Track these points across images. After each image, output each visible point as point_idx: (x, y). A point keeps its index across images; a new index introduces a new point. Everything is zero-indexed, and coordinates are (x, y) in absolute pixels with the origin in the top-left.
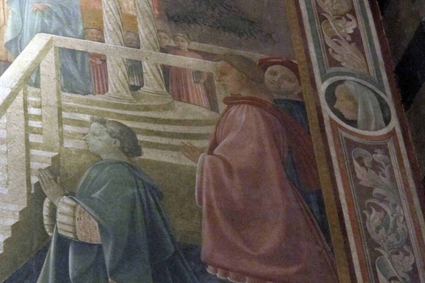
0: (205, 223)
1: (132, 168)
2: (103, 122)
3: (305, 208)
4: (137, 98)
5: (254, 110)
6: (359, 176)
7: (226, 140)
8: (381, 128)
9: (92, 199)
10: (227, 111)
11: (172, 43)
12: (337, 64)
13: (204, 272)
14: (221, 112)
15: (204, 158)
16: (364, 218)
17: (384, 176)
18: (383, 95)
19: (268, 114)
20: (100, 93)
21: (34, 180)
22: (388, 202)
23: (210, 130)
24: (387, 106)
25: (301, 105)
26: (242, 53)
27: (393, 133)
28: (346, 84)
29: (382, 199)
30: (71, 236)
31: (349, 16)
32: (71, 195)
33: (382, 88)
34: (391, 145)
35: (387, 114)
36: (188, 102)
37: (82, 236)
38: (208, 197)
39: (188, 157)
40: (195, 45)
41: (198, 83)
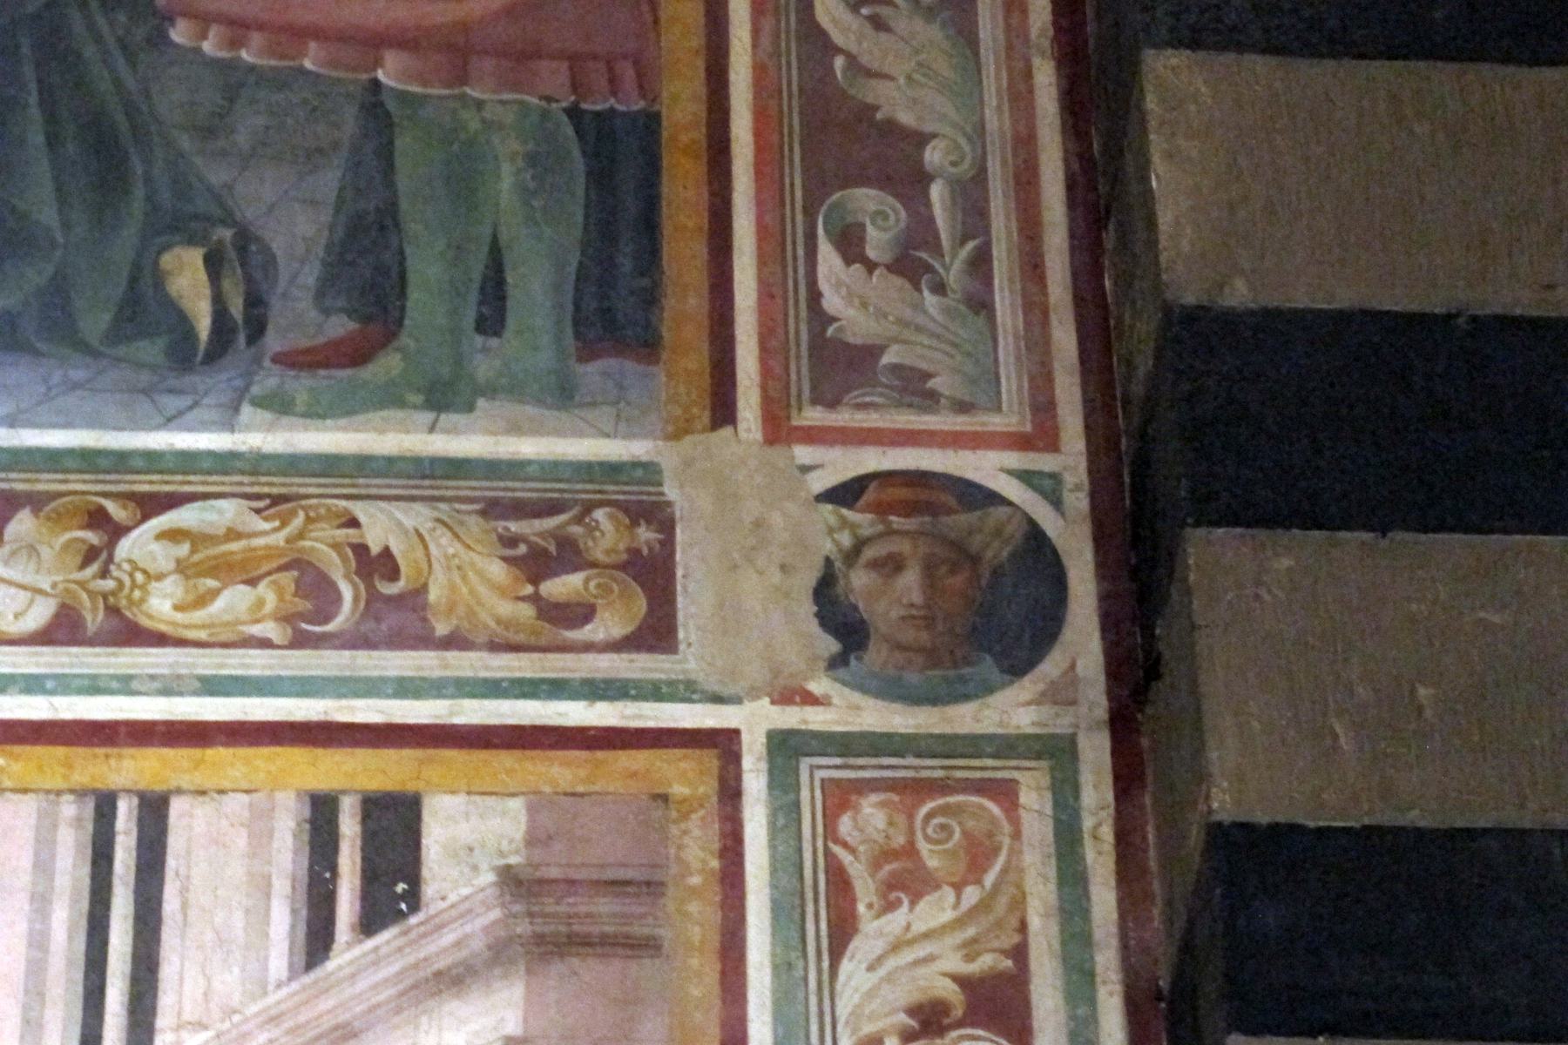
13: (159, 39)
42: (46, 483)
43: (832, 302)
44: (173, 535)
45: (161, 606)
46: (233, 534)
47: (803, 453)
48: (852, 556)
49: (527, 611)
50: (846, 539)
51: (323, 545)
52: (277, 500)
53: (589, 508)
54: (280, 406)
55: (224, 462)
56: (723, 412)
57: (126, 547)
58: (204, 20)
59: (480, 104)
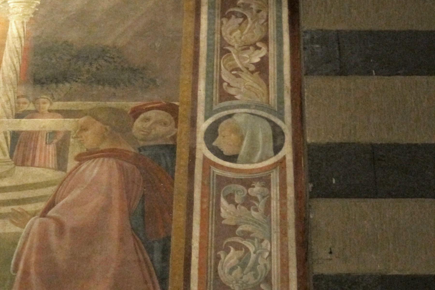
3: (145, 259)
5: (112, 162)
6: (223, 214)
7: (68, 198)
8: (268, 158)
10: (76, 168)
12: (232, 97)
14: (69, 170)
16: (218, 258)
17: (256, 210)
18: (279, 122)
22: (253, 238)
23: (49, 191)
24: (282, 134)
26: (113, 104)
27: (282, 161)
28: (235, 117)
29: (247, 235)
33: (281, 115)
35: (279, 142)
38: (26, 264)
40: (57, 105)
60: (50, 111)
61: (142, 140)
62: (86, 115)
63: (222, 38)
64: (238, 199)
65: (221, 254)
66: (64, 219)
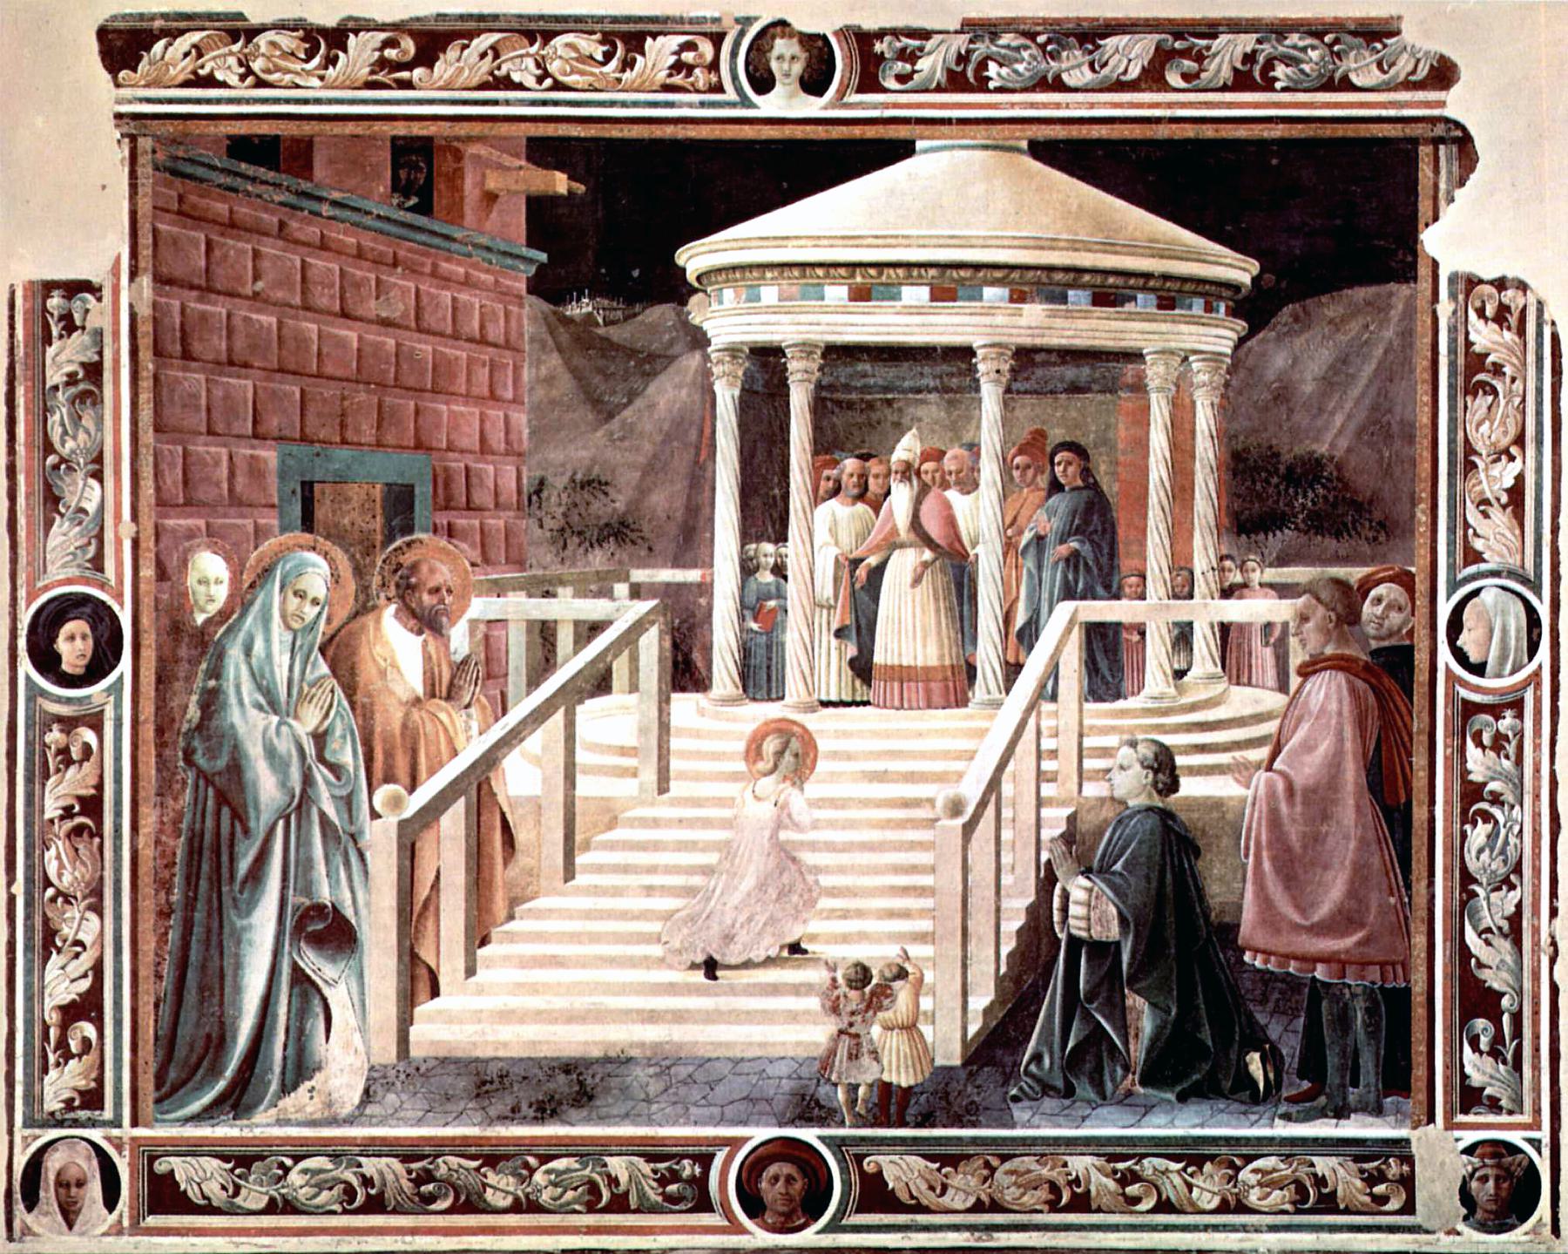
0: (1249, 887)
1: (1166, 815)
2: (1133, 744)
4: (1181, 690)
5: (1341, 677)
9: (1114, 873)
10: (1301, 686)
11: (1237, 577)
12: (1477, 557)
15: (1262, 776)
16: (1464, 836)
17: (1507, 757)
19: (1360, 684)
20: (1133, 694)
21: (1044, 856)
22: (1502, 804)
23: (1270, 727)
25: (1407, 653)
26: (1339, 571)
30: (1084, 934)
31: (1514, 450)
32: (1087, 872)
34: (1529, 697)
36: (1249, 684)
37: (1097, 933)
39: (1238, 781)
40: (1271, 574)
41: (1267, 644)
42: (1213, 1150)
43: (1468, 1070)
44: (1255, 1171)
45: (1253, 1198)
46: (1274, 1170)
47: (1457, 1134)
48: (1472, 1175)
49: (1367, 1199)
50: (1470, 1168)
51: (1303, 1173)
52: (1288, 1156)
53: (1388, 1157)
54: (1287, 1117)
55: (1270, 1141)
56: (1431, 1119)
57: (1241, 1176)
58: (1256, 951)
59: (1349, 986)
60: (1261, 585)
61: (1374, 638)
62: (1305, 592)
63: (1467, 440)
64: (1486, 738)
65: (1468, 827)
66: (1292, 773)
